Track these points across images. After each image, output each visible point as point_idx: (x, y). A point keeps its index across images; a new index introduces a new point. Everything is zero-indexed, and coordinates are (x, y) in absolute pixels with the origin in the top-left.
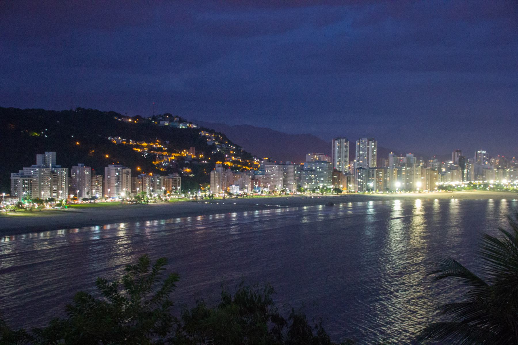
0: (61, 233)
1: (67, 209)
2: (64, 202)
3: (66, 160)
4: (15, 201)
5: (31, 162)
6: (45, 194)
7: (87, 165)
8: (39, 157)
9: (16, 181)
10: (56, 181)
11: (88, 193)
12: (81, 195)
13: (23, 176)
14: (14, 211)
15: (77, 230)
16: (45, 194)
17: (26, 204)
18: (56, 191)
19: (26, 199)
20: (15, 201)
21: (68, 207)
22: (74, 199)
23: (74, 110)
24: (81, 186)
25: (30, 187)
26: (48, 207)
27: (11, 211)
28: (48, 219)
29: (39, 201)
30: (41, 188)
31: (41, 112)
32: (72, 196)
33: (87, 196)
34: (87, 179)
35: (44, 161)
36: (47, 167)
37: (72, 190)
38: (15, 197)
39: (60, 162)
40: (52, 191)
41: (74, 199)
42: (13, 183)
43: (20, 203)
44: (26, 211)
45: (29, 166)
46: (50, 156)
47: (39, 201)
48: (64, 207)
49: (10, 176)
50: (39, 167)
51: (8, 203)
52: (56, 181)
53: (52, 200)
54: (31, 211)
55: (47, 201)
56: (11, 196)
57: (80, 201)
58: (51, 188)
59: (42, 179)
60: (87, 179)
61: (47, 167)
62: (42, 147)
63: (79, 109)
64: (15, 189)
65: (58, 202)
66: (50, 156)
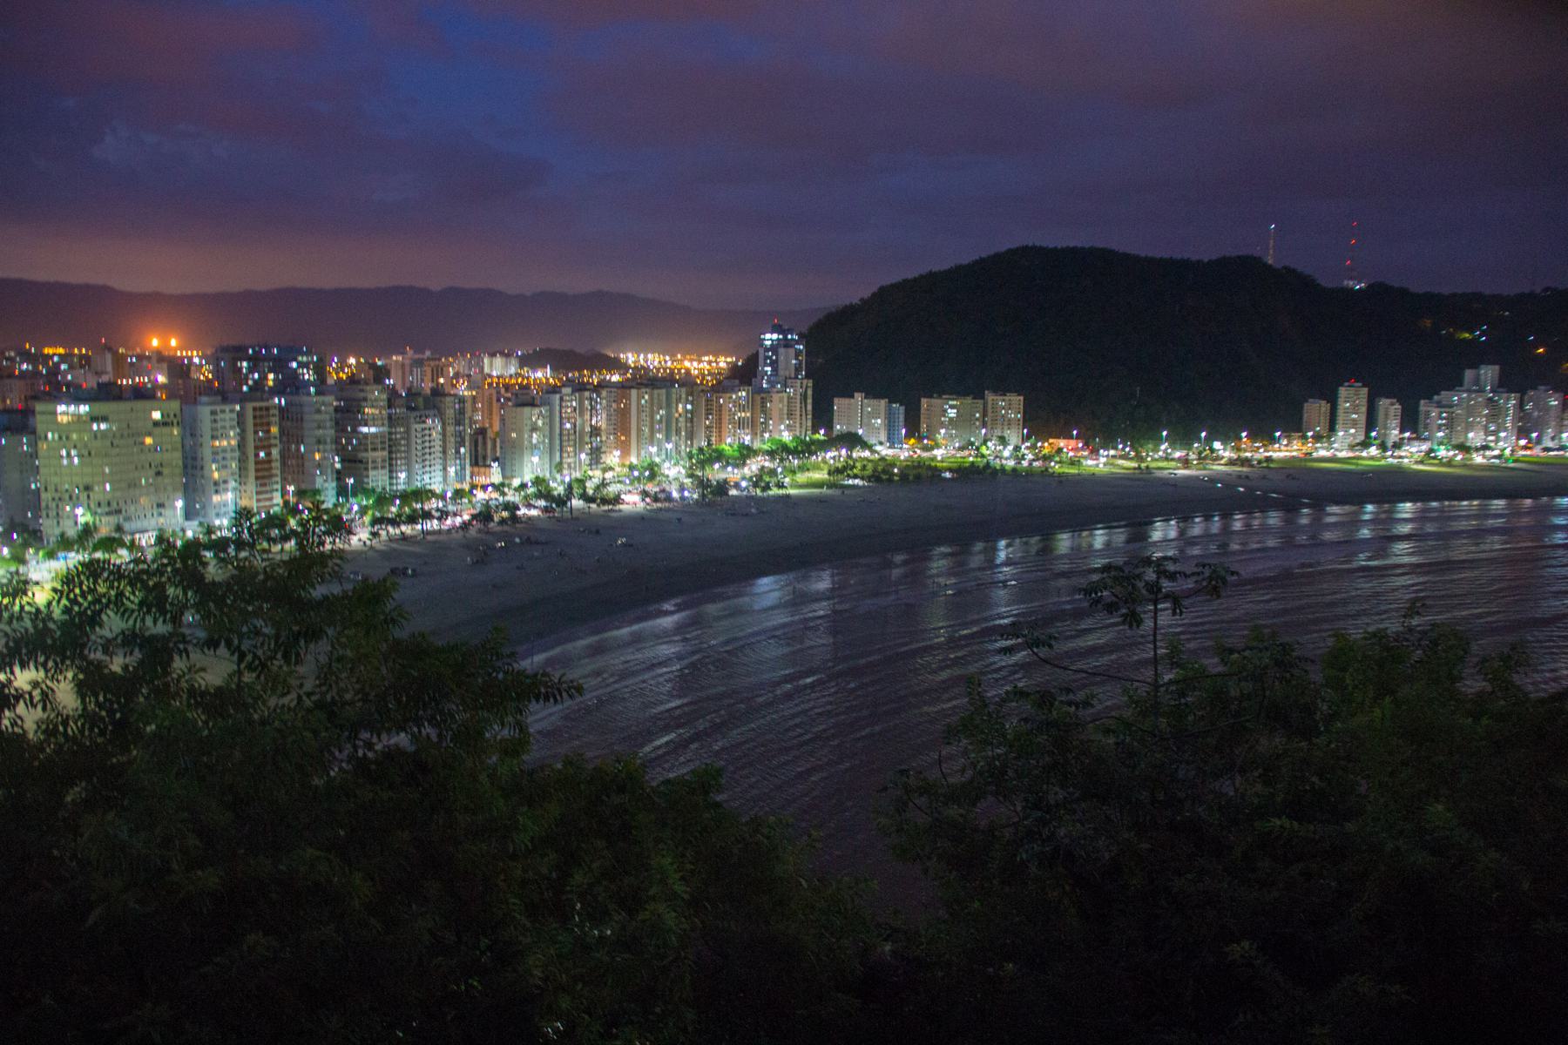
0: (1499, 504)
1: (1511, 465)
2: (1507, 452)
3: (1518, 380)
4: (1425, 447)
5: (1455, 383)
6: (1474, 437)
7: (1556, 390)
8: (1469, 374)
9: (1427, 413)
10: (1496, 414)
11: (1553, 439)
12: (1539, 440)
13: (1439, 405)
14: (1421, 462)
15: (1528, 502)
16: (1474, 437)
17: (1442, 452)
18: (1495, 433)
19: (1440, 444)
20: (1425, 447)
21: (1516, 461)
22: (1525, 448)
23: (1538, 290)
24: (1539, 425)
25: (1450, 425)
26: (1478, 459)
27: (1417, 462)
28: (1465, 478)
29: (1464, 448)
30: (1469, 427)
31: (1478, 296)
32: (1523, 442)
33: (1550, 444)
34: (1553, 413)
35: (1477, 381)
36: (1481, 391)
37: (1522, 432)
38: (1425, 439)
39: (1506, 384)
40: (1487, 433)
41: (1525, 448)
42: (1422, 417)
43: (1431, 450)
44: (1441, 464)
45: (1451, 388)
46: (1489, 373)
47: (1464, 448)
48: (1507, 460)
49: (1417, 405)
50: (1469, 391)
51: (1414, 450)
52: (1496, 414)
53: (1485, 448)
54: (1450, 463)
55: (1477, 449)
56: (1418, 438)
57: (1537, 451)
58: (1486, 428)
59: (1471, 411)
60: (1553, 413)
61: (1481, 391)
62: (1476, 356)
63: (1547, 289)
64: (1426, 427)
65: (1496, 452)
66: (1489, 373)
